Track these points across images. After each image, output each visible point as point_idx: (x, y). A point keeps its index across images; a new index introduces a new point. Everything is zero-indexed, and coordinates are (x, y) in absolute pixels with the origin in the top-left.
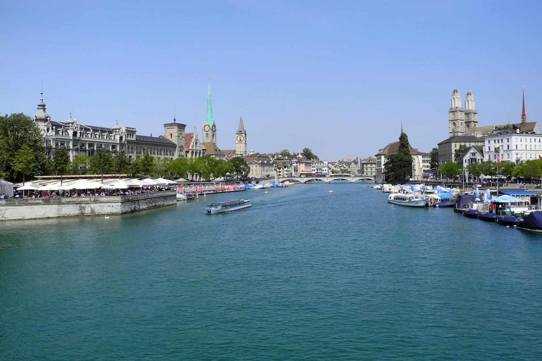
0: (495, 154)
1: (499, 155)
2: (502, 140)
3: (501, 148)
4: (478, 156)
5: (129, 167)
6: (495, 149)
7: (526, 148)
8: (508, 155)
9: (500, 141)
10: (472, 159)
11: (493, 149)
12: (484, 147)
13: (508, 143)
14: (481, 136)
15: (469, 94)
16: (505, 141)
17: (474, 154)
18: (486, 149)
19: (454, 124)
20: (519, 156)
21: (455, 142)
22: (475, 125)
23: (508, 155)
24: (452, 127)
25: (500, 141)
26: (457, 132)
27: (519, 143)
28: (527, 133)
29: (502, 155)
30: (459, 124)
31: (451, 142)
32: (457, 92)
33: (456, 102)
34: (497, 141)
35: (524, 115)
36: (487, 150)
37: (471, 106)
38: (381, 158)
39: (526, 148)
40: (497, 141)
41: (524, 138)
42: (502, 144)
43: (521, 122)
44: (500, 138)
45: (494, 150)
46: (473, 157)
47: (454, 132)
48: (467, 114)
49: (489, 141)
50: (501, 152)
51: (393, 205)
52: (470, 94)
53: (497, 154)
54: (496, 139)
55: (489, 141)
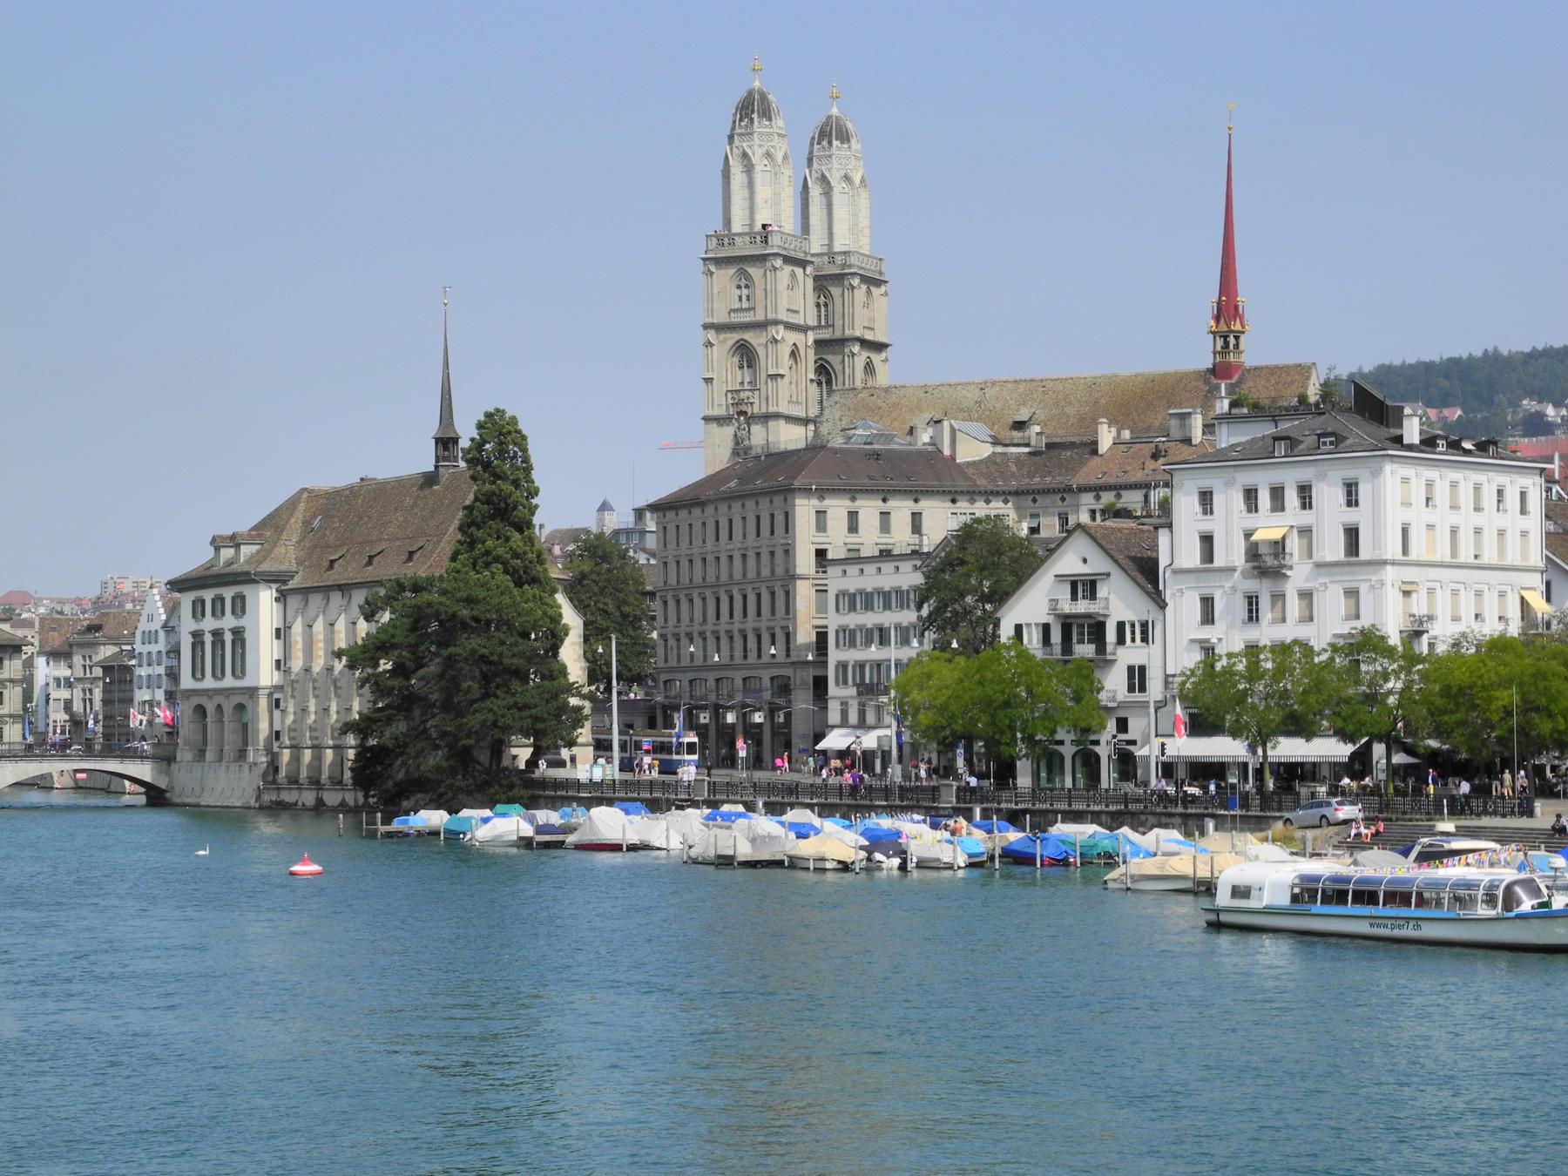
0: (1252, 585)
1: (1279, 598)
2: (1305, 493)
3: (1294, 545)
5: (631, 632)
6: (1253, 553)
7: (1454, 553)
8: (1352, 593)
9: (1292, 498)
10: (1067, 623)
11: (1231, 553)
13: (1351, 516)
14: (986, 450)
15: (830, 133)
16: (1329, 495)
17: (1084, 586)
18: (1178, 549)
19: (746, 355)
20: (1419, 606)
21: (822, 493)
22: (869, 368)
23: (1352, 593)
24: (729, 374)
25: (1292, 498)
26: (766, 418)
27: (1418, 517)
28: (1454, 446)
29: (1306, 596)
30: (776, 359)
31: (787, 492)
32: (766, 113)
33: (763, 192)
34: (1264, 498)
35: (1227, 310)
36: (1190, 556)
37: (851, 228)
38: (240, 605)
39: (1454, 553)
40: (1264, 498)
41: (1442, 478)
42: (1306, 518)
43: (1208, 363)
44: (1290, 478)
45: (1239, 559)
46: (1082, 606)
47: (741, 415)
48: (830, 282)
49: (1206, 498)
50: (1299, 575)
51: (1267, 941)
52: (845, 137)
53: (1264, 589)
54: (1263, 479)
55: (1206, 498)
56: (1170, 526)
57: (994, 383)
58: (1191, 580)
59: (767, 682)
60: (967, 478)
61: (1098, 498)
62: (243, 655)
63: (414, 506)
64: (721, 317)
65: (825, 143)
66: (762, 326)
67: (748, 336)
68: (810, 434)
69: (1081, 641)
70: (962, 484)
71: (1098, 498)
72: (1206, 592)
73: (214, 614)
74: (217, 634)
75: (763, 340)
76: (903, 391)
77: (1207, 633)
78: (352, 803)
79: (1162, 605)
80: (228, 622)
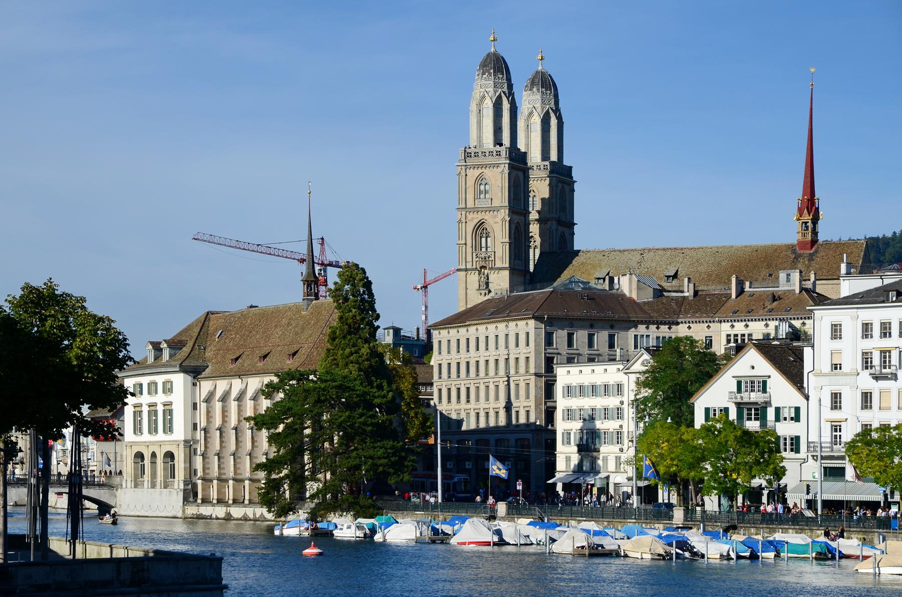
4: (781, 391)
12: (807, 351)
38: (168, 388)
56: (813, 347)
57: (649, 250)
58: (824, 381)
59: (512, 442)
60: (645, 313)
61: (733, 326)
62: (171, 421)
63: (289, 324)
64: (470, 204)
65: (535, 89)
66: (496, 209)
67: (487, 217)
68: (527, 281)
69: (749, 419)
70: (641, 316)
71: (733, 326)
72: (836, 389)
73: (149, 393)
74: (152, 405)
75: (499, 220)
76: (588, 254)
77: (836, 415)
78: (251, 516)
79: (807, 398)
80: (160, 398)
